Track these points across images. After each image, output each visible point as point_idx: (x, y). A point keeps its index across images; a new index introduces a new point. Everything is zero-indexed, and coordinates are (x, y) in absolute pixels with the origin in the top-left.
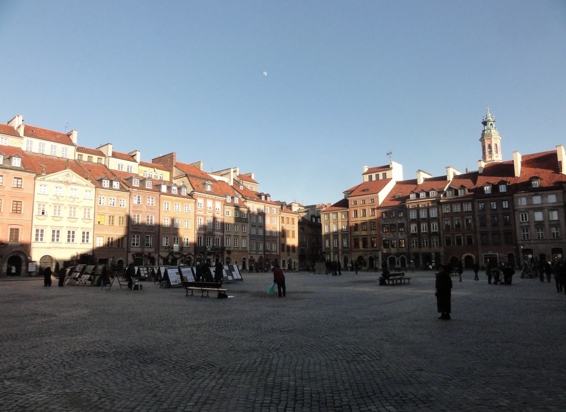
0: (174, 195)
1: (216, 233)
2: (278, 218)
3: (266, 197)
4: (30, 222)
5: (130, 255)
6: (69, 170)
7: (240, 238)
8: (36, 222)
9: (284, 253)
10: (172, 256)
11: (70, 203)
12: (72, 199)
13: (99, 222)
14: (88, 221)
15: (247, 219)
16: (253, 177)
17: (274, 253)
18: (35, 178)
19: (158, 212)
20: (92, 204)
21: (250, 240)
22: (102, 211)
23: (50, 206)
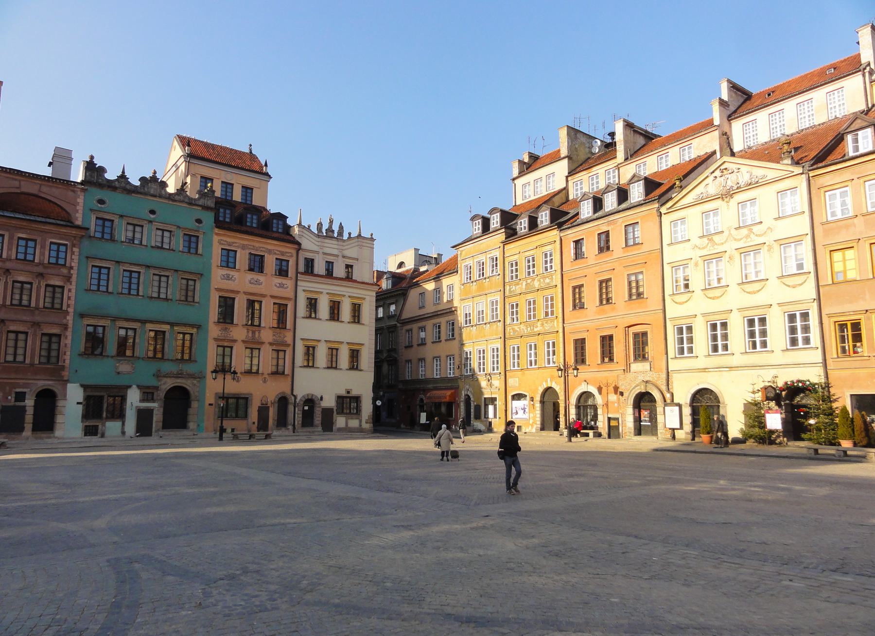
4: (662, 315)
11: (741, 244)
12: (744, 231)
14: (803, 278)
18: (661, 215)
20: (803, 225)
22: (843, 237)
23: (696, 265)
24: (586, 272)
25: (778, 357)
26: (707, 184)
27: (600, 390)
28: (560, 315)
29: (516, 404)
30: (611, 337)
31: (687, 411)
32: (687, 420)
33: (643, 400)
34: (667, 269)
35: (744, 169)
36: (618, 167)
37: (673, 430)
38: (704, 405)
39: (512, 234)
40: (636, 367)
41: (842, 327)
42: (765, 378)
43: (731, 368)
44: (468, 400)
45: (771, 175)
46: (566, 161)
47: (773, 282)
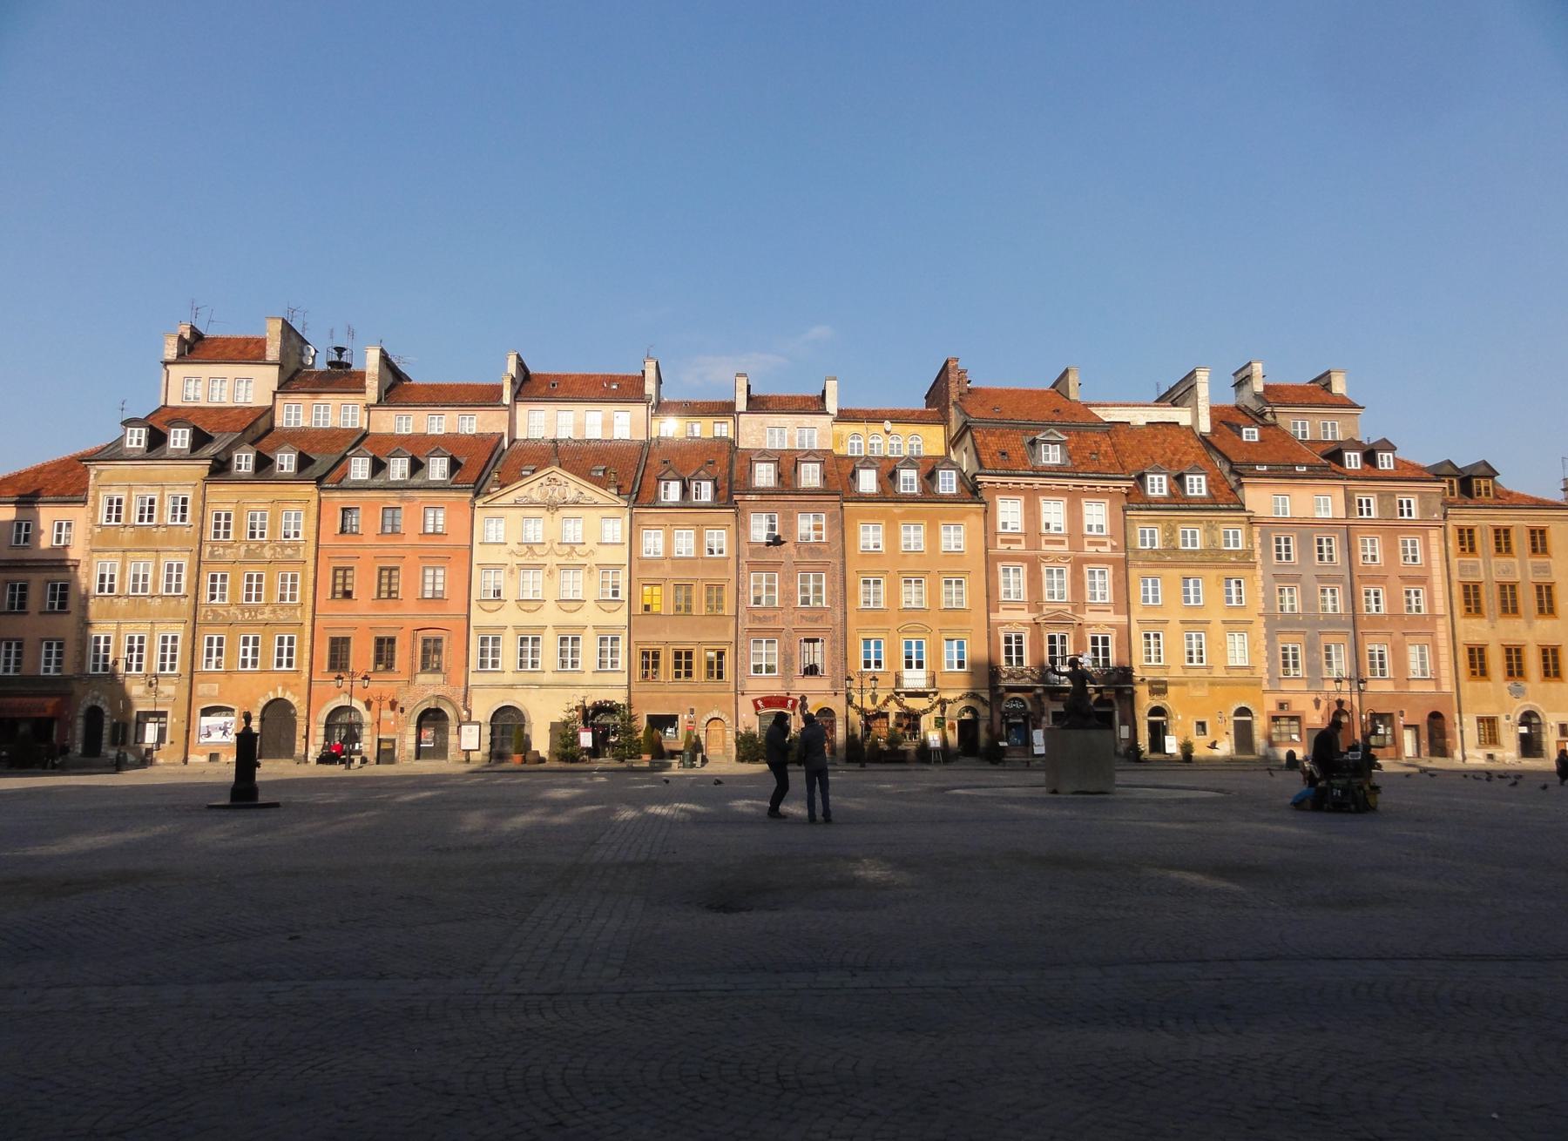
0: (912, 499)
1: (1089, 617)
2: (1434, 534)
3: (1370, 456)
5: (746, 705)
6: (555, 468)
7: (1217, 628)
8: (478, 617)
9: (1480, 684)
10: (900, 704)
11: (562, 561)
12: (567, 549)
13: (647, 608)
14: (614, 606)
15: (1249, 553)
16: (1339, 386)
17: (1415, 688)
19: (837, 561)
20: (622, 556)
21: (1270, 637)
22: (654, 574)
23: (512, 572)
24: (359, 552)
25: (588, 678)
26: (533, 488)
27: (368, 704)
28: (310, 602)
29: (206, 721)
30: (392, 641)
31: (487, 730)
32: (487, 740)
33: (432, 718)
34: (475, 569)
35: (571, 484)
36: (368, 407)
37: (468, 751)
38: (507, 725)
39: (220, 469)
40: (422, 678)
41: (645, 654)
42: (576, 698)
43: (541, 686)
44: (94, 715)
45: (597, 498)
46: (276, 368)
47: (590, 604)
